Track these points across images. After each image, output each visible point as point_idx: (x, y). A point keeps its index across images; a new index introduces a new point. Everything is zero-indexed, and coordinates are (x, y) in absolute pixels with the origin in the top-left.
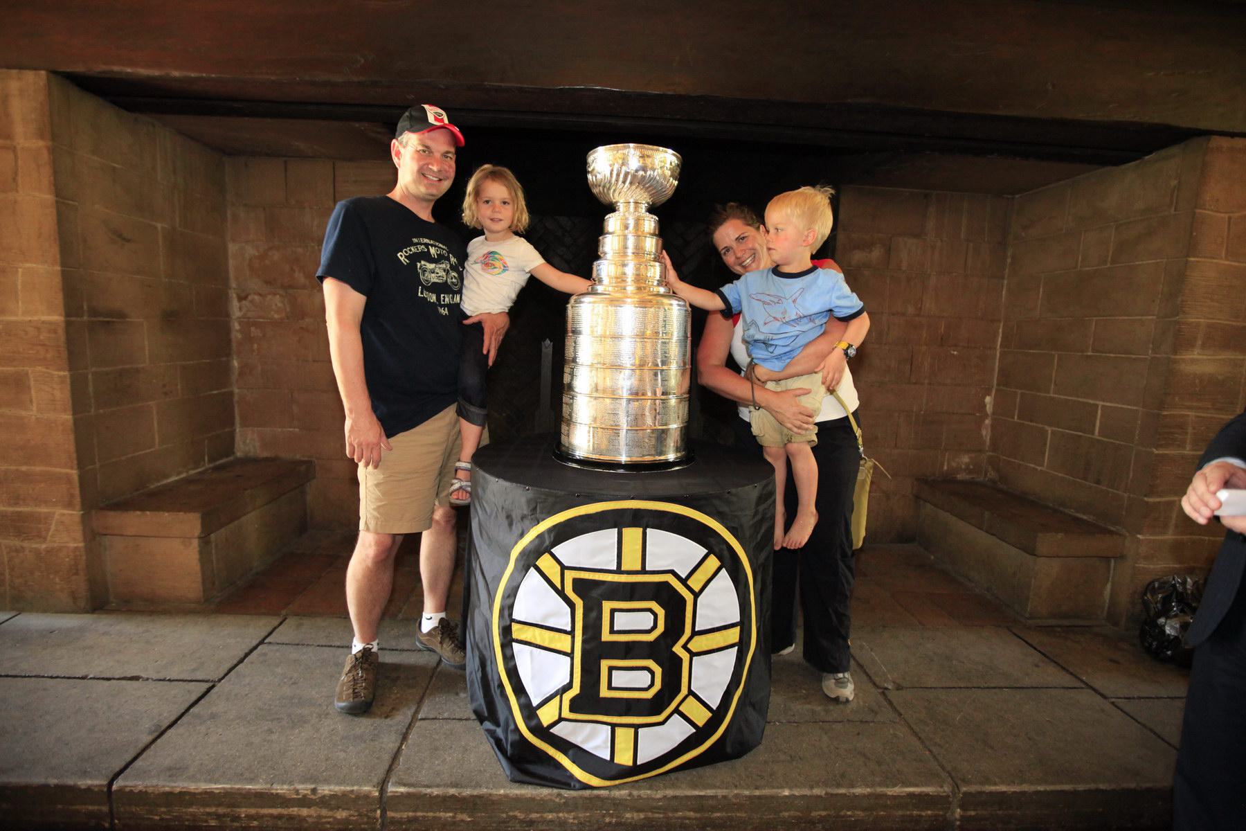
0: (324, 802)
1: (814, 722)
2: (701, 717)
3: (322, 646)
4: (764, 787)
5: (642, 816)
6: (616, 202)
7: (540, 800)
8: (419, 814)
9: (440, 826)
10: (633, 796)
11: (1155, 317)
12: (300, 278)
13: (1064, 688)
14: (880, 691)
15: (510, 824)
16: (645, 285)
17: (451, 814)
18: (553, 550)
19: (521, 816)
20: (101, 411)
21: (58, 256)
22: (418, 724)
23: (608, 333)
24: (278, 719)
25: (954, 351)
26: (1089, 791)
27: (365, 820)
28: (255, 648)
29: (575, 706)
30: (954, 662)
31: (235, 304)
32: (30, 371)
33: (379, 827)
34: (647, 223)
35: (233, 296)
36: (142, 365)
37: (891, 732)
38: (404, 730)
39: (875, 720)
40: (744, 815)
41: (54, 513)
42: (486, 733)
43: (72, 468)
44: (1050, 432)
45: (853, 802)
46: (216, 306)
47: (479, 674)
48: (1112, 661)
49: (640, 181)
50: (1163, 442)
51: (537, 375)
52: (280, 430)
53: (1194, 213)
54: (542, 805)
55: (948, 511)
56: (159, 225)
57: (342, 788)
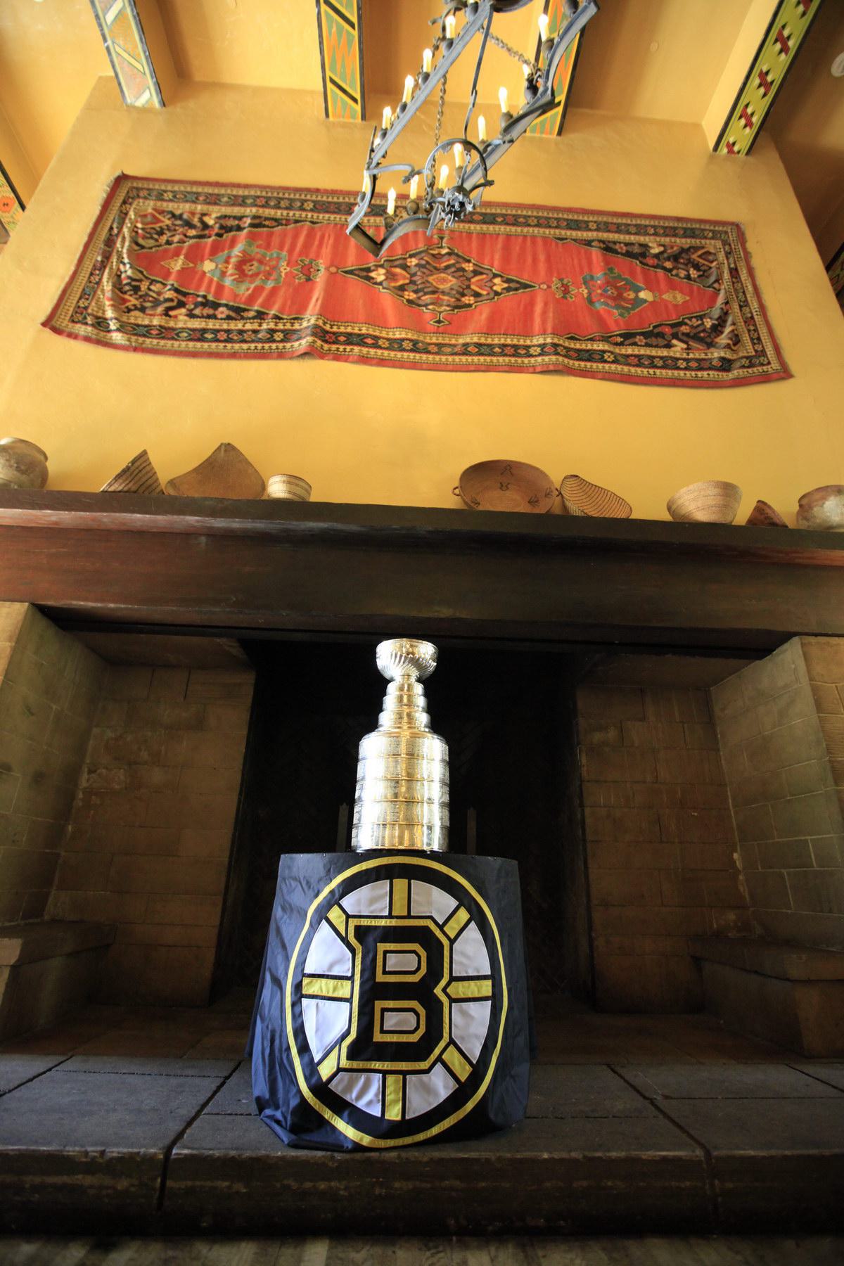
5: (410, 1185)
12: (144, 755)
19: (294, 1185)
25: (694, 812)
29: (353, 1053)
31: (85, 776)
36: (7, 813)
40: (508, 1185)
46: (72, 774)
47: (267, 1051)
56: (54, 707)
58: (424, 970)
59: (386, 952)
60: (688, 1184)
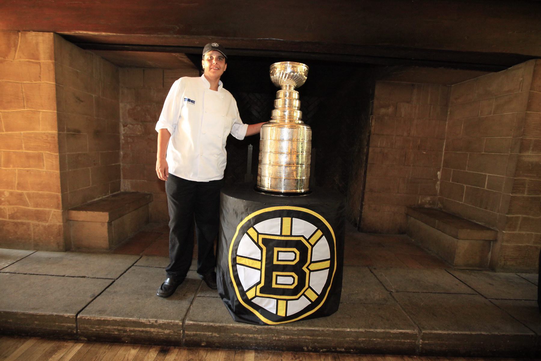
0: (160, 326)
1: (361, 303)
2: (314, 297)
3: (157, 267)
4: (339, 327)
5: (288, 337)
6: (281, 86)
7: (247, 329)
8: (198, 333)
9: (206, 338)
10: (285, 329)
11: (512, 137)
13: (468, 294)
14: (389, 292)
15: (233, 339)
16: (292, 120)
17: (211, 333)
18: (254, 226)
19: (239, 335)
20: (70, 170)
21: (56, 107)
22: (196, 298)
23: (277, 139)
24: (141, 294)
25: (424, 152)
26: (478, 335)
27: (176, 334)
28: (131, 267)
29: (262, 291)
30: (421, 282)
31: (122, 128)
32: (43, 154)
33: (182, 337)
34: (294, 94)
35: (121, 125)
37: (393, 308)
38: (191, 301)
39: (387, 304)
40: (331, 338)
41: (51, 211)
42: (224, 303)
43: (59, 193)
44: (465, 187)
45: (376, 335)
46: (115, 128)
48: (490, 284)
49: (292, 77)
50: (515, 191)
51: (246, 160)
52: (139, 181)
53: (530, 92)
54: (248, 331)
55: (419, 220)
56: (94, 96)
57: (167, 321)
58: (298, 259)
59: (278, 252)
60: (408, 341)
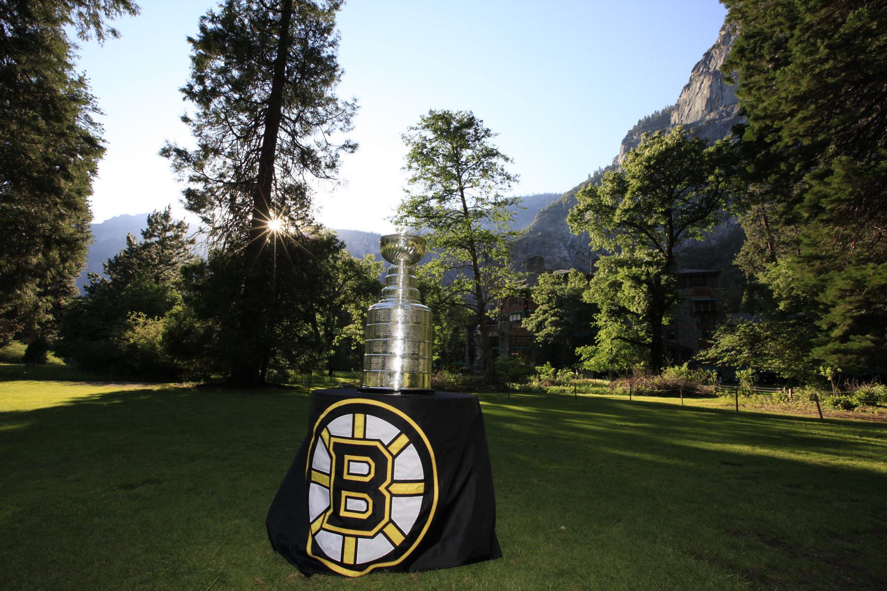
2: (399, 539)
58: (372, 475)
59: (349, 461)
